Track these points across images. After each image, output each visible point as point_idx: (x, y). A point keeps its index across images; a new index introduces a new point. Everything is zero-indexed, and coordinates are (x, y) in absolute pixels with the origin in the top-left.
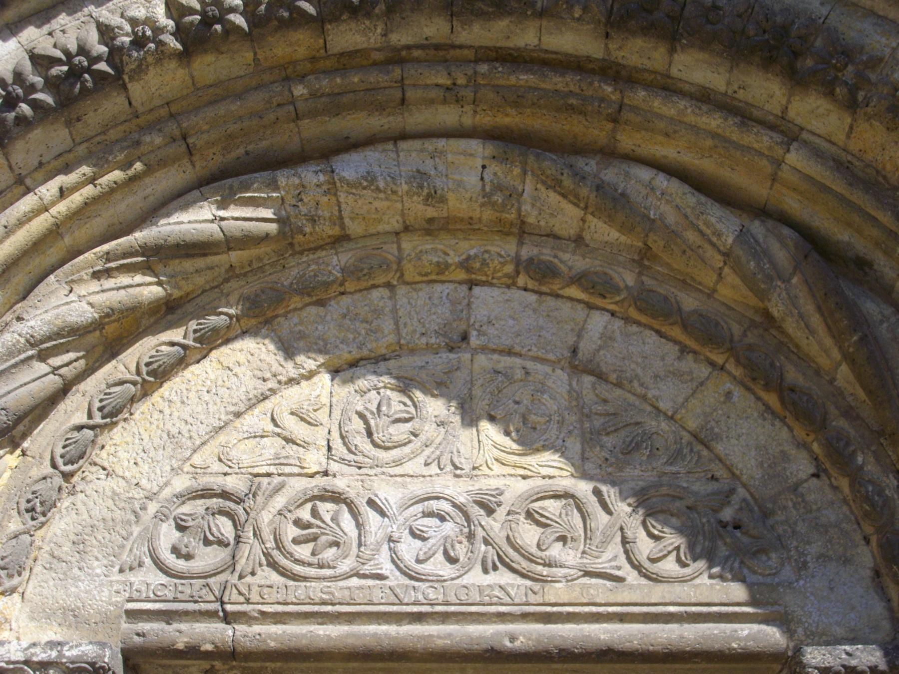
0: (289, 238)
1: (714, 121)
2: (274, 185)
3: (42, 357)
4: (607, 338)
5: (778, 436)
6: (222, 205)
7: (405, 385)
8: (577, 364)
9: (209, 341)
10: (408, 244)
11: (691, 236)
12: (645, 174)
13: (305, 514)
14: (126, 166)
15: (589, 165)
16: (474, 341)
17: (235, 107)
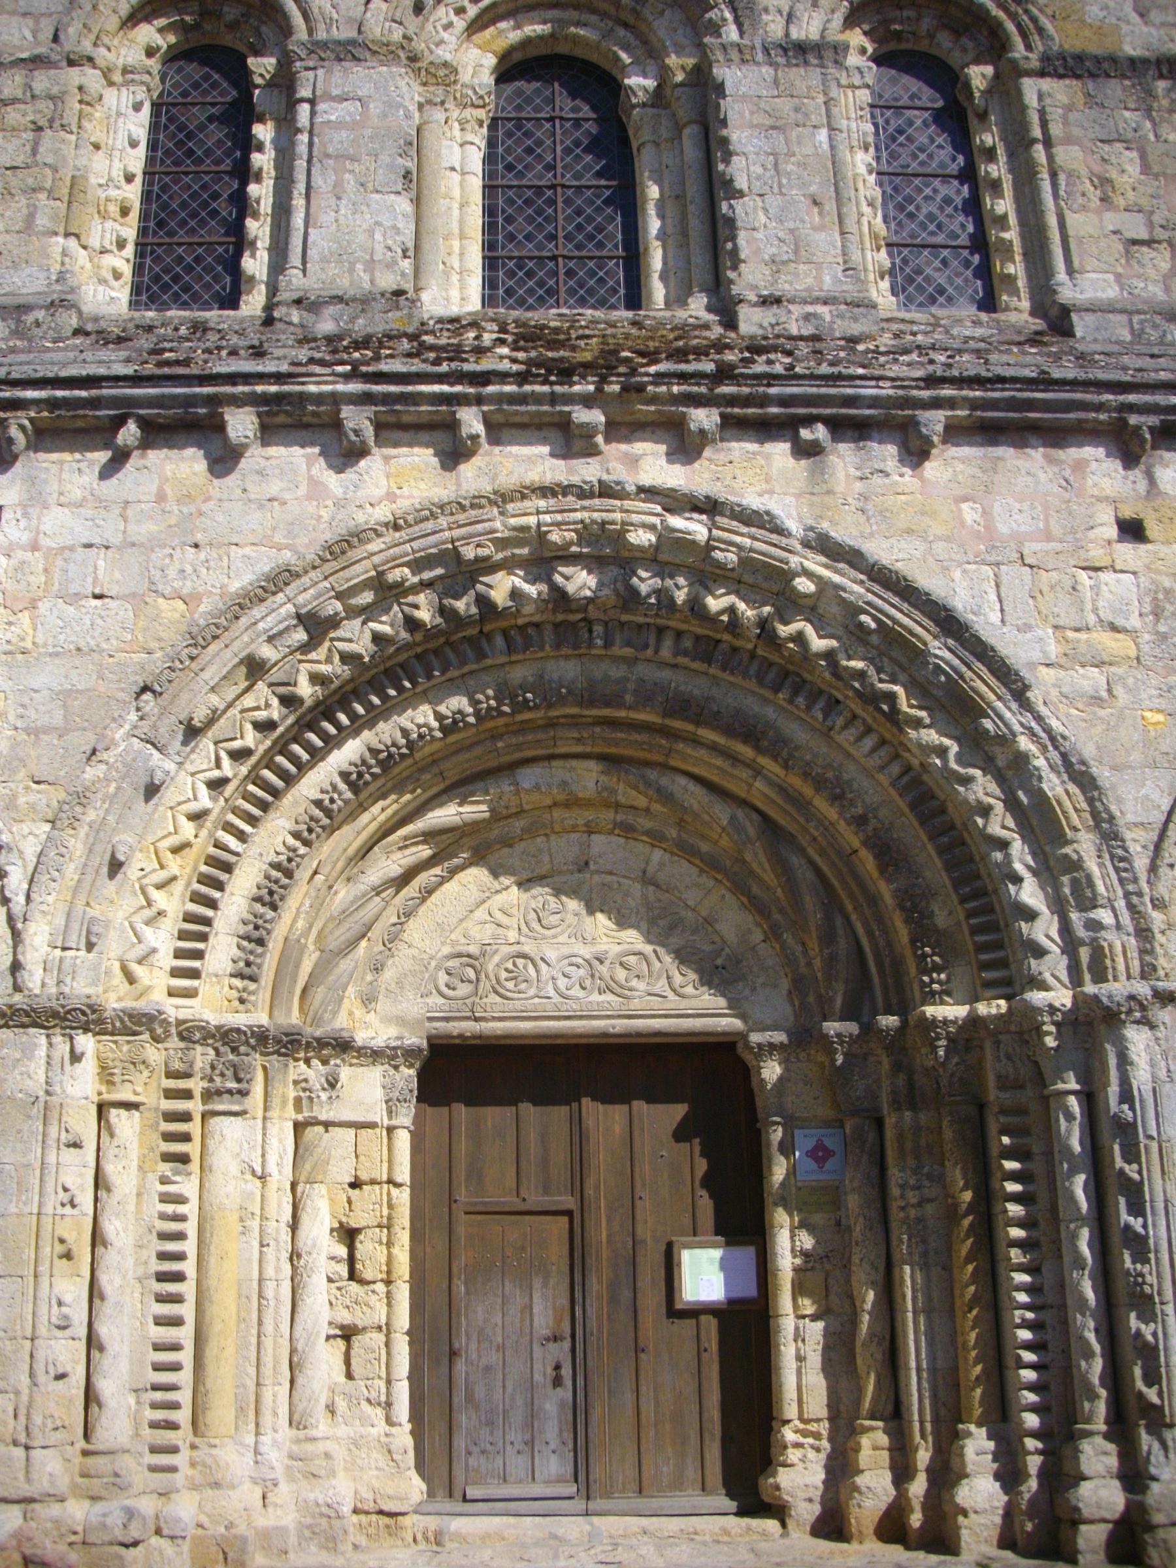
0: (496, 816)
1: (719, 762)
2: (487, 793)
4: (662, 864)
5: (747, 919)
6: (461, 804)
7: (557, 892)
8: (647, 880)
9: (453, 872)
10: (557, 814)
11: (706, 817)
12: (682, 781)
13: (510, 965)
14: (413, 791)
15: (652, 774)
16: (592, 867)
17: (467, 756)
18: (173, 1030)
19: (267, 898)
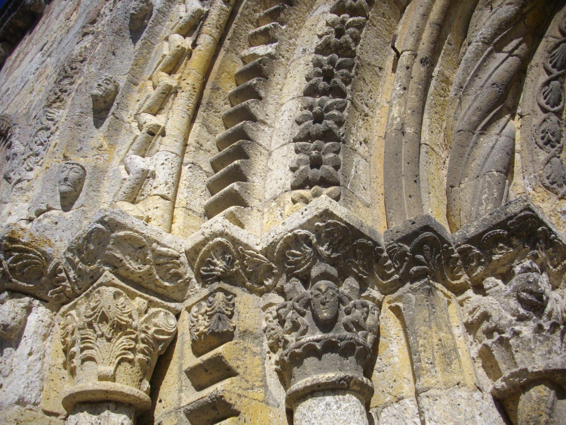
3: (498, 48)
18: (190, 274)
19: (322, 84)
